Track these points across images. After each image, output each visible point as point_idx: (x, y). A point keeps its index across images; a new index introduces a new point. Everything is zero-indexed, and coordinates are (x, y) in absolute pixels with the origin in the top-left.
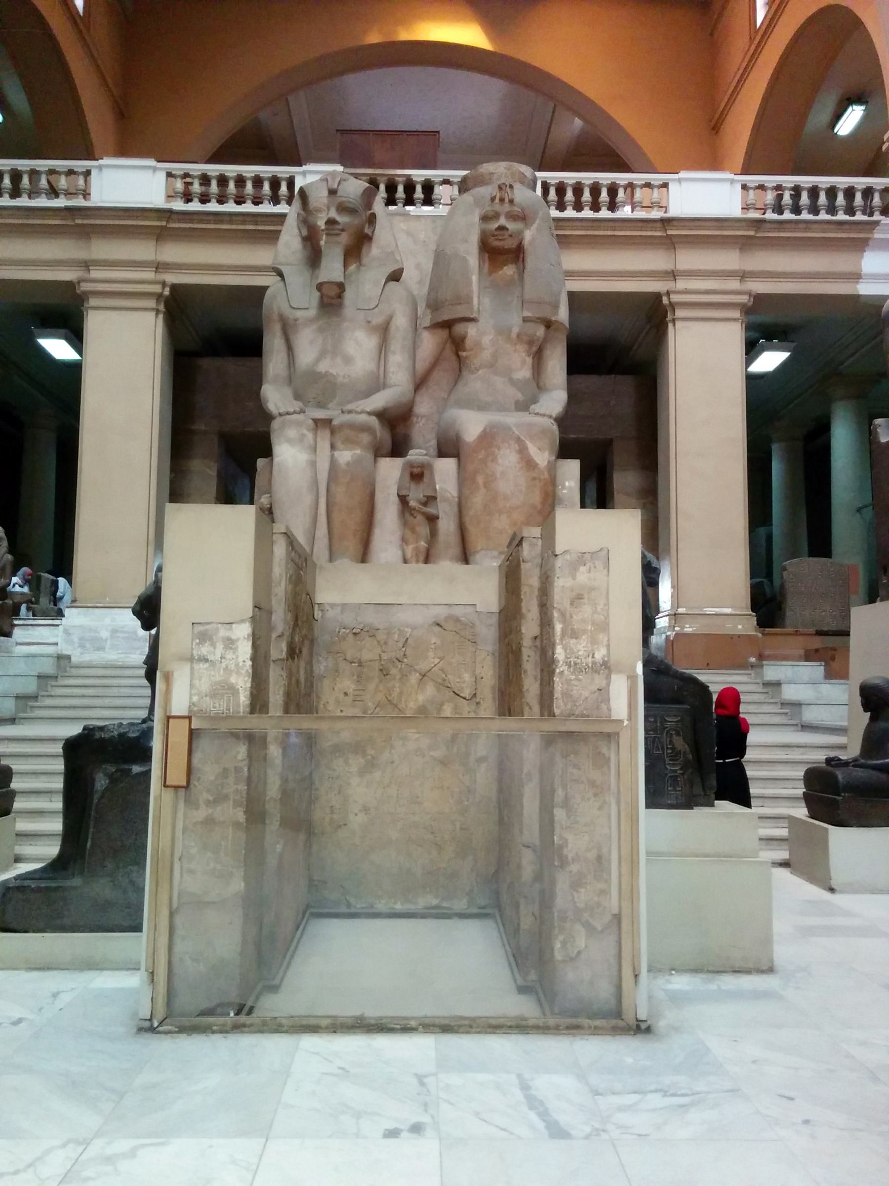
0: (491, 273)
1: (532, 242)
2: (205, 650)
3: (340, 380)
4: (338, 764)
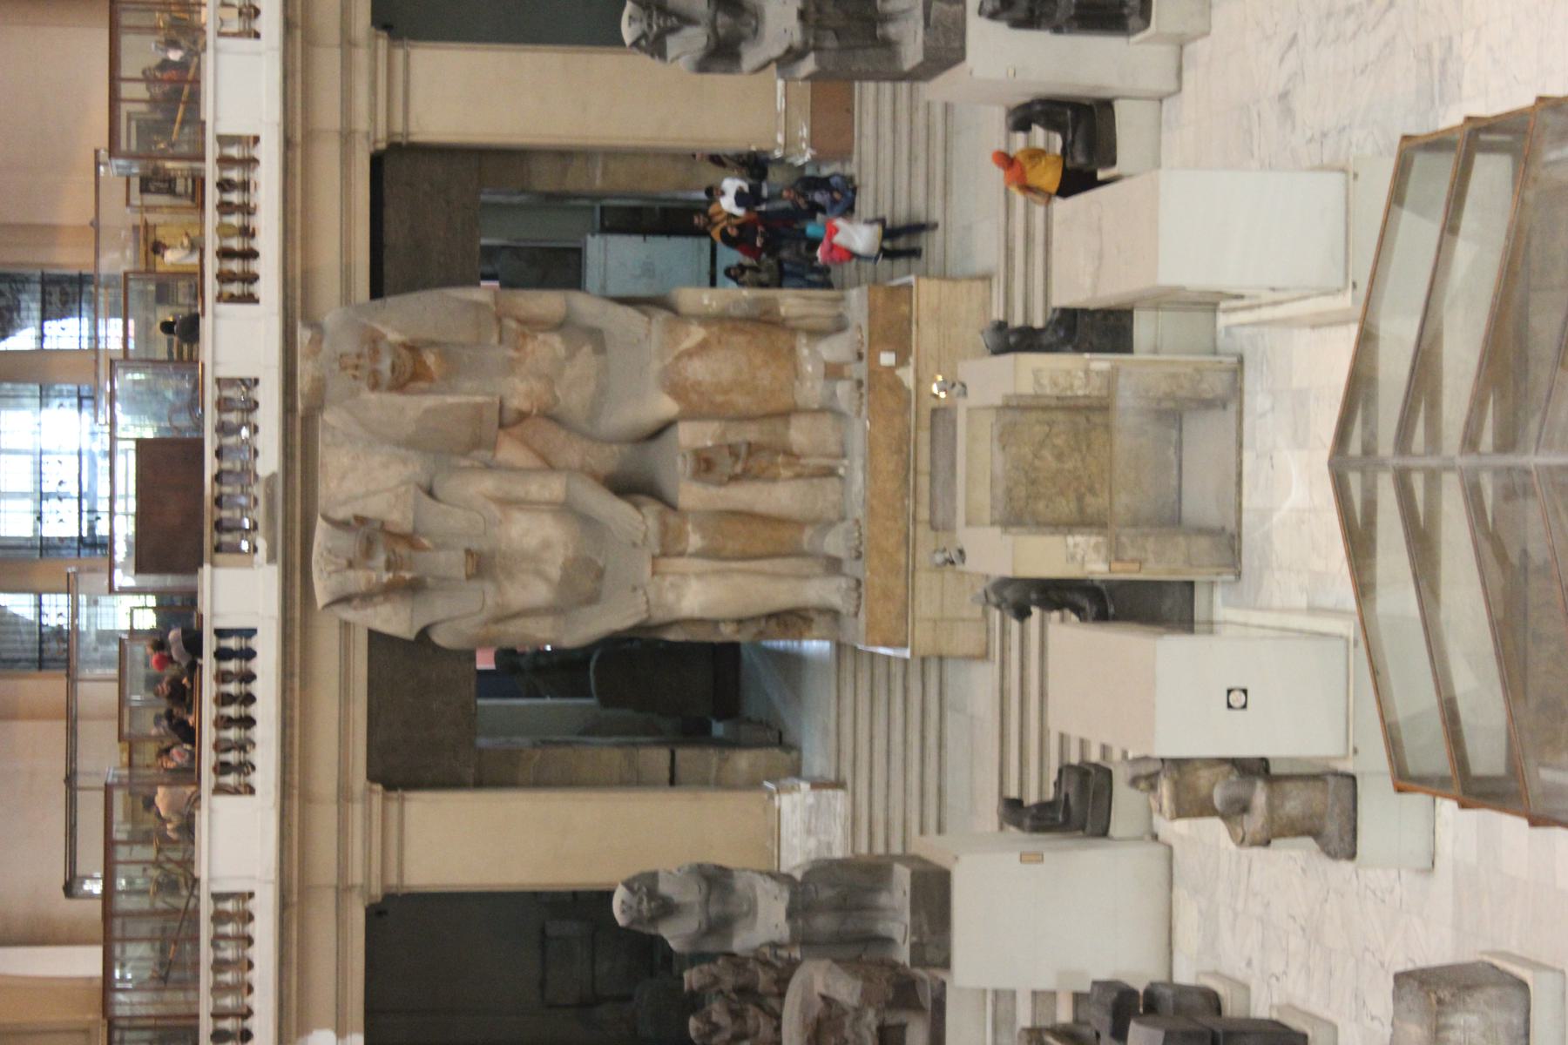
0: (432, 380)
1: (400, 331)
2: (1079, 557)
3: (570, 553)
4: (1089, 511)
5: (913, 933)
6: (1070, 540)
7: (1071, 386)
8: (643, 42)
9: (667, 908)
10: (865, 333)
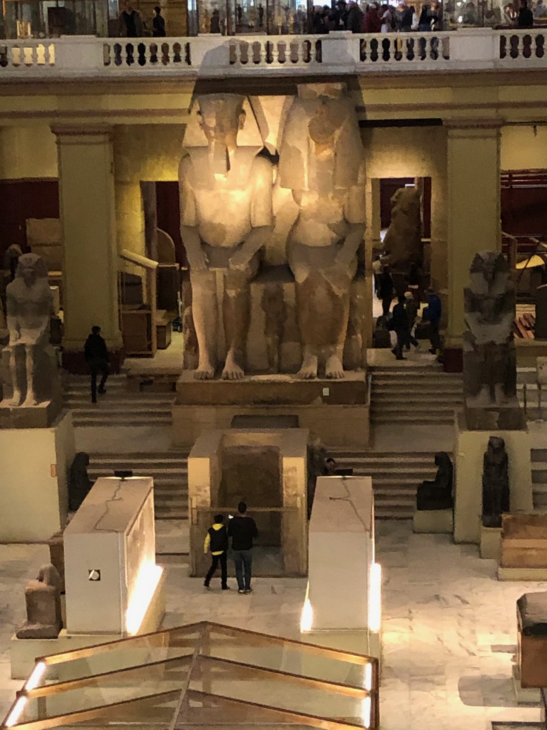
0: (316, 153)
3: (228, 229)
5: (14, 410)
6: (208, 488)
7: (287, 487)
8: (480, 261)
9: (30, 281)
10: (341, 380)
